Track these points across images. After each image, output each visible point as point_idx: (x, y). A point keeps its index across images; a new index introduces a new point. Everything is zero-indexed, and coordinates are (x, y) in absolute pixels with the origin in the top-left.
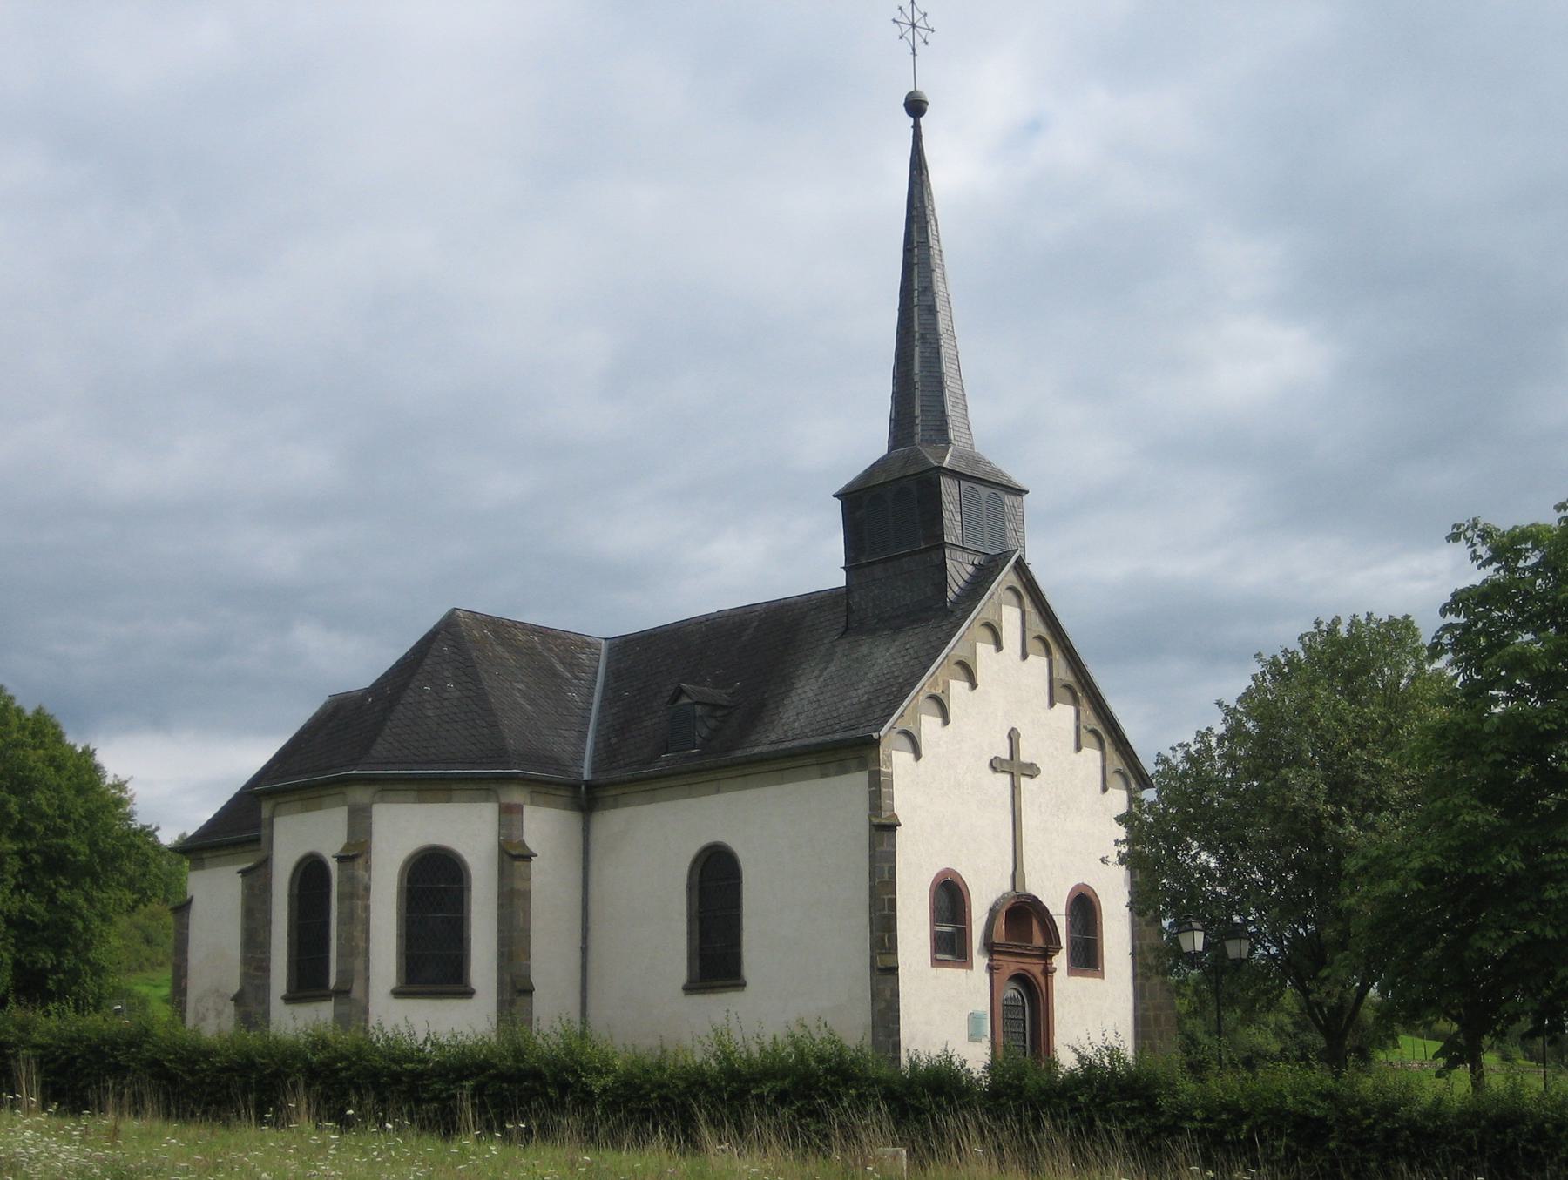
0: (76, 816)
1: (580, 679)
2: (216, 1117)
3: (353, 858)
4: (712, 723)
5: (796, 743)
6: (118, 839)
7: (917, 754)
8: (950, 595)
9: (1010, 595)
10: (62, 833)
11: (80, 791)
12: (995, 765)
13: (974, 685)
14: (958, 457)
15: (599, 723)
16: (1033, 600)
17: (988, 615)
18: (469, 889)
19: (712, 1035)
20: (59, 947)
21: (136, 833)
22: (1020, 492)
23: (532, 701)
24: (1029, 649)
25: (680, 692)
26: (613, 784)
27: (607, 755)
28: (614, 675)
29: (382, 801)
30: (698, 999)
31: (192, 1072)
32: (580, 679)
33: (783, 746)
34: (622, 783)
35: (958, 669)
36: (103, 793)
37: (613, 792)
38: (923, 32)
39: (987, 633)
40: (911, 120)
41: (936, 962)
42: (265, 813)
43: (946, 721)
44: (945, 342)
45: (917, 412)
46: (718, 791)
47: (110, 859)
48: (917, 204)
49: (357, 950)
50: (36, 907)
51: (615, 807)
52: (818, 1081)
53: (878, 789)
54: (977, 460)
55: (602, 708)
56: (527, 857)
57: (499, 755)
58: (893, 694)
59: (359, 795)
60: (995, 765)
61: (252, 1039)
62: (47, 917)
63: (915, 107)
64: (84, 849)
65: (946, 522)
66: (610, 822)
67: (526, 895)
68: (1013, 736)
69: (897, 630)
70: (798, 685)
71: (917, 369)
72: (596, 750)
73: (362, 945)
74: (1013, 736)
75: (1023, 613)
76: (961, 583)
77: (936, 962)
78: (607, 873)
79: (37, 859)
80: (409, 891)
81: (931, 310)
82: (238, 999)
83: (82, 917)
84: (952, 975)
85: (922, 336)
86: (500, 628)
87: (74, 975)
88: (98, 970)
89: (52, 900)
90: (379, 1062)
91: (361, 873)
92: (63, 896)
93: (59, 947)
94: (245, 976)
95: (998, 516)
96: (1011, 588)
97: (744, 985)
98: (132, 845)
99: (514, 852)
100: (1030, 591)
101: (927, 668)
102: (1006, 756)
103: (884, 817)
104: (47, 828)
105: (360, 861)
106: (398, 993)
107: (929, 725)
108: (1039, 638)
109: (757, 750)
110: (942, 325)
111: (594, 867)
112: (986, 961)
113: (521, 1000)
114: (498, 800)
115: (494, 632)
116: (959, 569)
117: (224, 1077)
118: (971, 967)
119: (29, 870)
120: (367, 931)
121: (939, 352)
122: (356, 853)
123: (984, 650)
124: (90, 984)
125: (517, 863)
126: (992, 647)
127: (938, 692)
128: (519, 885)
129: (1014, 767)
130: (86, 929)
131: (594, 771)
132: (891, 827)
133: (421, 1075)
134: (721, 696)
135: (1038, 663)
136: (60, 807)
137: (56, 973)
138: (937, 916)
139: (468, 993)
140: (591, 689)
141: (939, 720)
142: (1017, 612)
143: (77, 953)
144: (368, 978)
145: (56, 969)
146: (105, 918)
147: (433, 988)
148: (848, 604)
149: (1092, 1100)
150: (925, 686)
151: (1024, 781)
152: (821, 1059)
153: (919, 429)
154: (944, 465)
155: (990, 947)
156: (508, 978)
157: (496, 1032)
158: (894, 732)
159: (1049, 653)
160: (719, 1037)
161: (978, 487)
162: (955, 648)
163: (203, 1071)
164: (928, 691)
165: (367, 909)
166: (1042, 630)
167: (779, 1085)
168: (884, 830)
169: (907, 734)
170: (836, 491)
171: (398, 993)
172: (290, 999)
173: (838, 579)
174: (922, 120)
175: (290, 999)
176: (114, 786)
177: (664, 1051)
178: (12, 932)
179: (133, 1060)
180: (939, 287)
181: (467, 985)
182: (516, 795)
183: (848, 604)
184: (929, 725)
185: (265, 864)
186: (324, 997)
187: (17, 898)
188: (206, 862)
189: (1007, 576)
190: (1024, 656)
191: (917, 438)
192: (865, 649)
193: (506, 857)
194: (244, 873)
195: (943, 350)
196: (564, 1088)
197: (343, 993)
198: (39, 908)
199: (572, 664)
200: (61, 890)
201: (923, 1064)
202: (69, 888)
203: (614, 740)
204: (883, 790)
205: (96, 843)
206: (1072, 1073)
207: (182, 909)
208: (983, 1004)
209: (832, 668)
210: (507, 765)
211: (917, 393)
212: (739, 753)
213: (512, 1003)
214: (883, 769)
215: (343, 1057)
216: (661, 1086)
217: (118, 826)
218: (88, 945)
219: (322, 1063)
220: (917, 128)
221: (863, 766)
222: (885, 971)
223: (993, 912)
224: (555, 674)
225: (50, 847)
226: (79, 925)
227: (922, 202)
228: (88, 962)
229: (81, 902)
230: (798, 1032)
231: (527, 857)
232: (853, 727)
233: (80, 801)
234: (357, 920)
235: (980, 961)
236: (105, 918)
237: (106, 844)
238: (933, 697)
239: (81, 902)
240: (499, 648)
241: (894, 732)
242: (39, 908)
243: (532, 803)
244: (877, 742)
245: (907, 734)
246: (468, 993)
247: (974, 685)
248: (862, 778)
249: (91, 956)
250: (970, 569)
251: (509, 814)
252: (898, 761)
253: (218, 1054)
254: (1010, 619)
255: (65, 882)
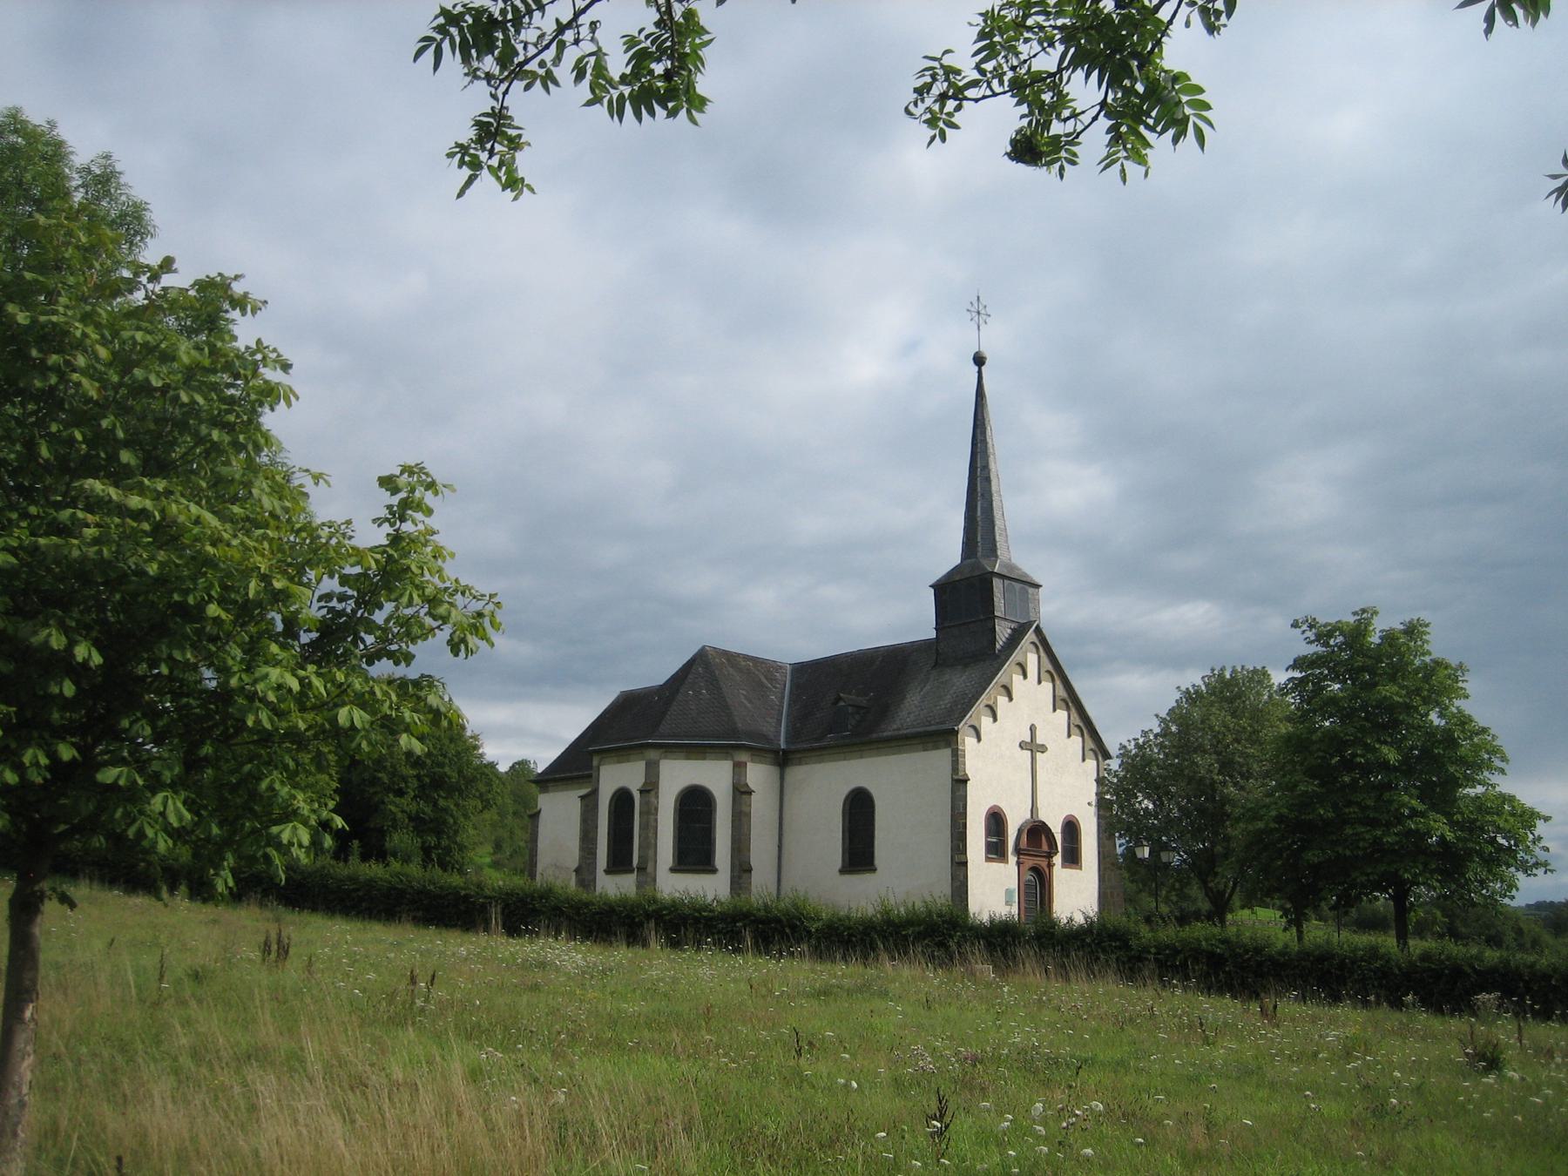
0: (450, 755)
1: (776, 688)
2: (605, 941)
3: (648, 791)
4: (857, 717)
5: (908, 731)
6: (475, 769)
7: (979, 739)
8: (998, 646)
9: (1032, 647)
10: (442, 765)
11: (451, 740)
12: (1022, 746)
13: (1011, 699)
14: (1003, 565)
15: (788, 715)
16: (1044, 650)
17: (1020, 659)
18: (715, 811)
19: (879, 900)
20: (439, 834)
21: (485, 766)
22: (1038, 586)
23: (750, 702)
24: (1042, 678)
25: (839, 699)
26: (798, 751)
27: (793, 735)
28: (797, 687)
29: (666, 758)
30: (847, 877)
31: (578, 914)
32: (776, 688)
33: (901, 732)
34: (805, 750)
35: (1002, 690)
36: (465, 742)
37: (799, 756)
38: (985, 317)
39: (1018, 669)
40: (976, 368)
41: (988, 859)
42: (595, 763)
43: (995, 720)
44: (995, 498)
45: (979, 539)
46: (862, 757)
47: (471, 781)
48: (980, 418)
49: (650, 844)
50: (426, 809)
51: (800, 764)
52: (939, 927)
53: (957, 758)
54: (1012, 567)
55: (789, 705)
56: (750, 793)
57: (734, 733)
58: (965, 704)
59: (652, 754)
60: (1022, 746)
61: (585, 896)
62: (432, 816)
63: (979, 360)
64: (455, 775)
65: (996, 604)
66: (796, 773)
67: (749, 815)
68: (1033, 729)
69: (966, 666)
70: (908, 696)
71: (979, 513)
72: (787, 732)
73: (653, 841)
74: (1033, 729)
75: (1039, 657)
76: (1004, 639)
77: (988, 859)
78: (794, 803)
79: (427, 780)
80: (680, 810)
81: (988, 480)
82: (577, 871)
83: (452, 816)
84: (996, 866)
85: (982, 495)
86: (731, 657)
87: (448, 850)
88: (462, 848)
89: (435, 804)
90: (687, 911)
91: (653, 799)
92: (442, 803)
93: (439, 834)
94: (582, 858)
95: (1025, 600)
96: (1033, 643)
97: (875, 870)
98: (483, 773)
99: (742, 790)
100: (1043, 644)
101: (985, 689)
102: (1029, 740)
103: (960, 776)
104: (433, 762)
105: (653, 793)
106: (673, 870)
107: (986, 722)
108: (1048, 672)
109: (885, 734)
110: (994, 488)
111: (786, 798)
112: (1016, 859)
113: (745, 876)
114: (732, 760)
115: (728, 660)
116: (1003, 632)
117: (597, 917)
118: (1007, 862)
119: (422, 787)
120: (656, 834)
121: (992, 505)
122: (650, 788)
123: (1017, 678)
124: (457, 856)
125: (744, 796)
126: (1021, 677)
127: (991, 703)
128: (744, 808)
129: (1033, 746)
130: (455, 823)
131: (787, 742)
132: (964, 781)
133: (711, 919)
134: (863, 701)
135: (1047, 686)
136: (441, 749)
137: (437, 849)
138: (989, 833)
139: (714, 871)
140: (783, 693)
141: (991, 719)
142: (1036, 656)
143: (448, 837)
144: (656, 862)
145: (437, 847)
146: (466, 816)
147: (694, 867)
148: (937, 649)
149: (1093, 941)
150: (984, 700)
151: (1039, 755)
152: (940, 915)
153: (980, 549)
154: (996, 571)
155: (1018, 851)
156: (737, 863)
157: (1234, 939)
158: (966, 727)
159: (1053, 681)
160: (883, 902)
161: (1027, 587)
162: (1000, 678)
163: (584, 913)
164: (985, 702)
165: (656, 820)
166: (1050, 667)
167: (917, 929)
168: (960, 783)
169: (974, 727)
170: (931, 583)
171: (673, 870)
172: (608, 872)
173: (933, 635)
174: (983, 368)
175: (608, 872)
176: (471, 737)
177: (850, 909)
178: (412, 824)
179: (545, 906)
180: (992, 466)
181: (714, 866)
182: (743, 757)
183: (937, 649)
184: (986, 722)
185: (594, 793)
186: (632, 871)
187: (414, 804)
188: (550, 789)
189: (1030, 636)
190: (1039, 682)
191: (979, 554)
192: (947, 677)
193: (737, 793)
194: (582, 798)
195: (994, 503)
196: (793, 928)
197: (642, 869)
198: (428, 810)
199: (772, 680)
200: (441, 800)
201: (997, 919)
202: (446, 798)
203: (798, 725)
204: (960, 759)
205: (462, 772)
206: (1081, 926)
207: (535, 816)
208: (1014, 885)
209: (928, 687)
210: (739, 739)
211: (979, 528)
212: (874, 736)
213: (740, 877)
214: (960, 747)
215: (665, 908)
216: (849, 928)
217: (476, 762)
218: (456, 832)
219: (654, 911)
220: (980, 373)
221: (948, 745)
222: (959, 865)
223: (1020, 831)
224: (762, 685)
225: (434, 773)
226: (451, 821)
227: (983, 416)
228: (456, 843)
229: (452, 806)
230: (929, 899)
231: (750, 793)
232: (942, 723)
233: (452, 746)
234: (650, 828)
235: (1012, 859)
236: (466, 816)
237: (468, 772)
238: (988, 706)
239: (452, 806)
240: (731, 670)
241: (966, 727)
242: (428, 810)
243: (752, 761)
244: (957, 732)
245: (974, 727)
246: (714, 871)
247: (1011, 699)
248: (947, 752)
249: (458, 839)
250: (1009, 631)
251: (739, 768)
252: (968, 743)
253: (593, 904)
254: (1032, 661)
255: (444, 795)
